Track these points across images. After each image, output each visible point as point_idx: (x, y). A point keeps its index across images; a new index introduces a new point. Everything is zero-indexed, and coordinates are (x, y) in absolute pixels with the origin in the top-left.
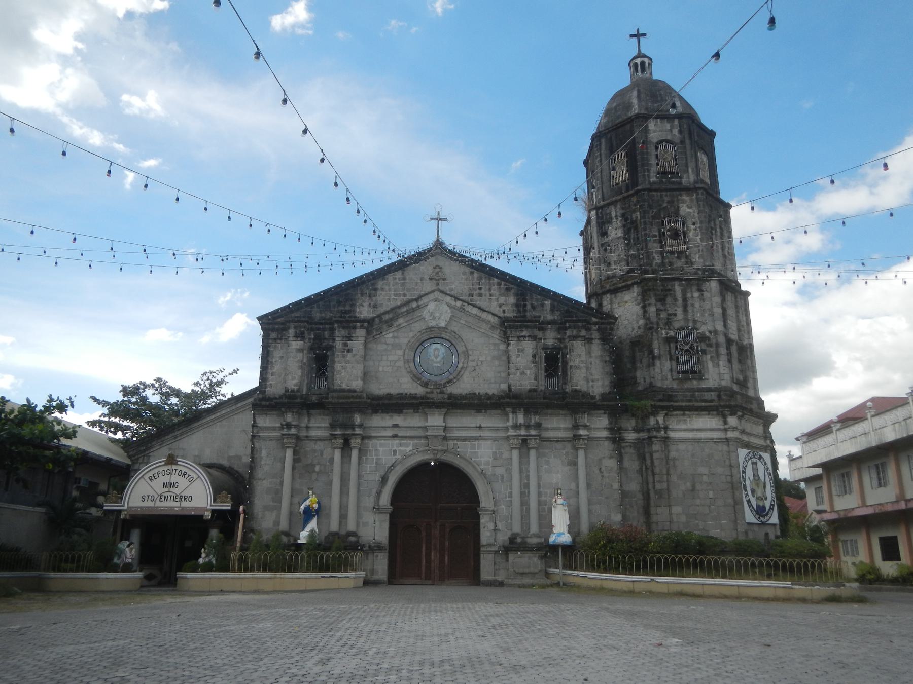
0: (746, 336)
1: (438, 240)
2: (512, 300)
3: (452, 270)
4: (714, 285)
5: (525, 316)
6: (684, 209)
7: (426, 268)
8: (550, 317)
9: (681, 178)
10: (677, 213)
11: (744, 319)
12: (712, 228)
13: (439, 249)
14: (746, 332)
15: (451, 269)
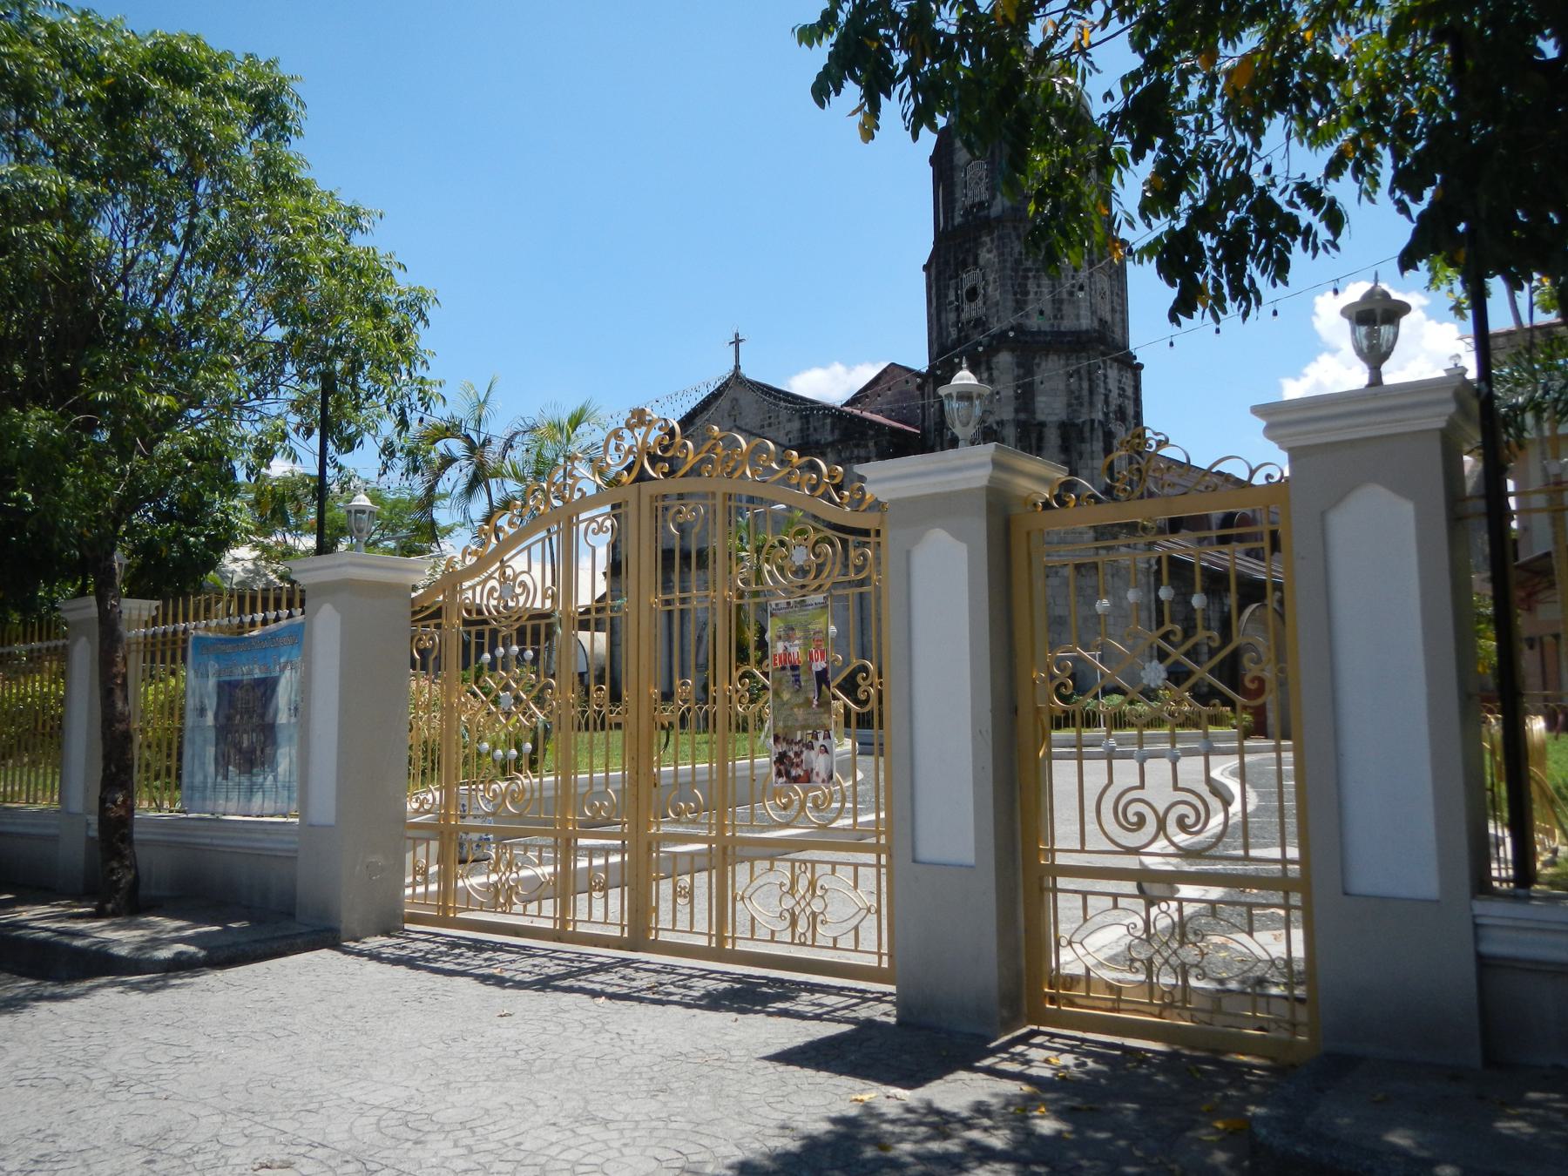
0: (1085, 410)
1: (737, 367)
2: (796, 425)
3: (747, 399)
4: (1004, 359)
5: (807, 443)
6: (985, 256)
7: (723, 402)
8: (830, 439)
9: (990, 207)
10: (976, 263)
11: (1085, 385)
12: (1028, 270)
13: (737, 379)
14: (1086, 404)
15: (747, 399)
